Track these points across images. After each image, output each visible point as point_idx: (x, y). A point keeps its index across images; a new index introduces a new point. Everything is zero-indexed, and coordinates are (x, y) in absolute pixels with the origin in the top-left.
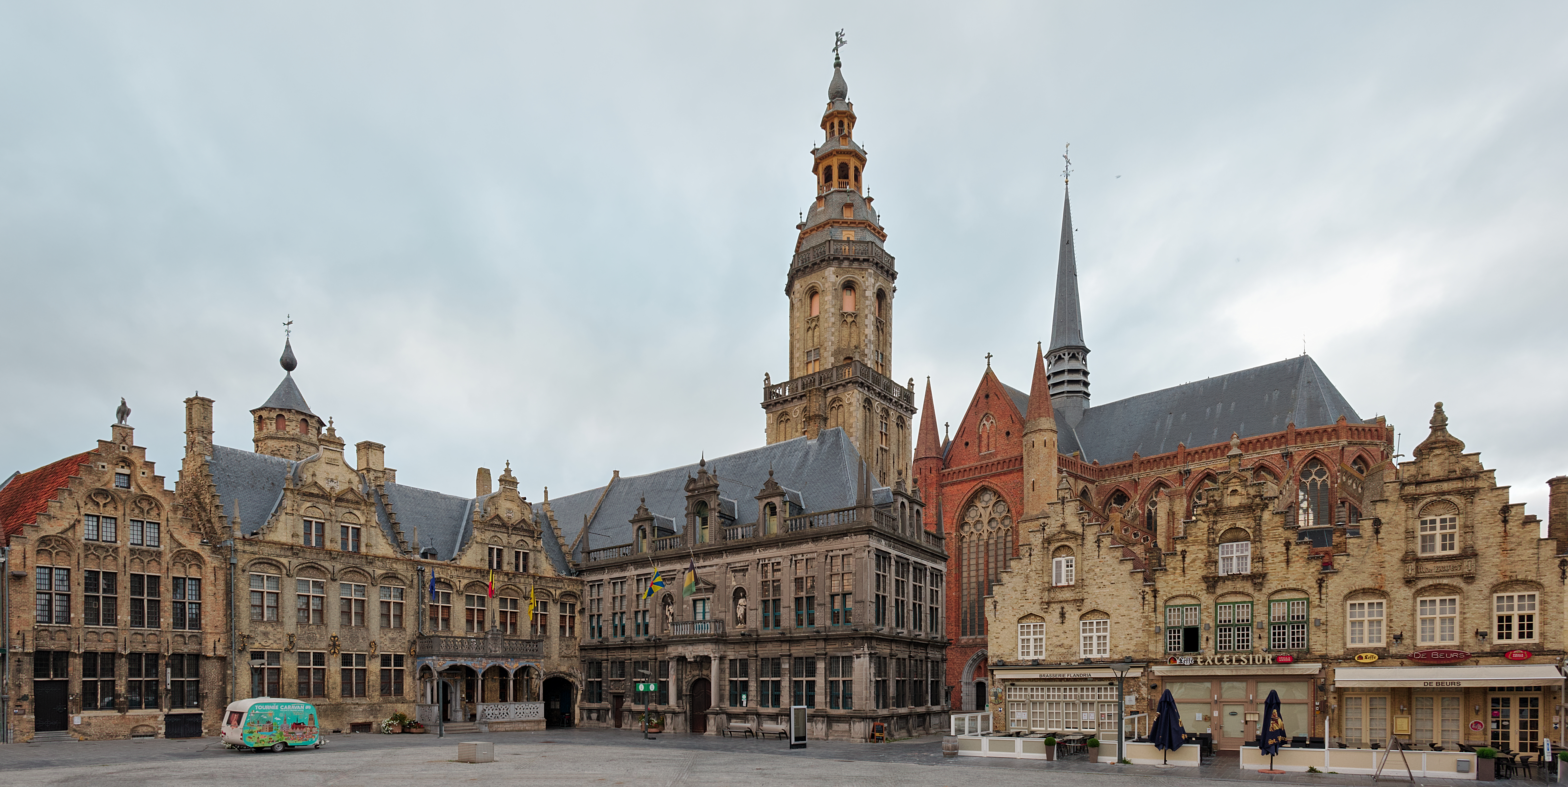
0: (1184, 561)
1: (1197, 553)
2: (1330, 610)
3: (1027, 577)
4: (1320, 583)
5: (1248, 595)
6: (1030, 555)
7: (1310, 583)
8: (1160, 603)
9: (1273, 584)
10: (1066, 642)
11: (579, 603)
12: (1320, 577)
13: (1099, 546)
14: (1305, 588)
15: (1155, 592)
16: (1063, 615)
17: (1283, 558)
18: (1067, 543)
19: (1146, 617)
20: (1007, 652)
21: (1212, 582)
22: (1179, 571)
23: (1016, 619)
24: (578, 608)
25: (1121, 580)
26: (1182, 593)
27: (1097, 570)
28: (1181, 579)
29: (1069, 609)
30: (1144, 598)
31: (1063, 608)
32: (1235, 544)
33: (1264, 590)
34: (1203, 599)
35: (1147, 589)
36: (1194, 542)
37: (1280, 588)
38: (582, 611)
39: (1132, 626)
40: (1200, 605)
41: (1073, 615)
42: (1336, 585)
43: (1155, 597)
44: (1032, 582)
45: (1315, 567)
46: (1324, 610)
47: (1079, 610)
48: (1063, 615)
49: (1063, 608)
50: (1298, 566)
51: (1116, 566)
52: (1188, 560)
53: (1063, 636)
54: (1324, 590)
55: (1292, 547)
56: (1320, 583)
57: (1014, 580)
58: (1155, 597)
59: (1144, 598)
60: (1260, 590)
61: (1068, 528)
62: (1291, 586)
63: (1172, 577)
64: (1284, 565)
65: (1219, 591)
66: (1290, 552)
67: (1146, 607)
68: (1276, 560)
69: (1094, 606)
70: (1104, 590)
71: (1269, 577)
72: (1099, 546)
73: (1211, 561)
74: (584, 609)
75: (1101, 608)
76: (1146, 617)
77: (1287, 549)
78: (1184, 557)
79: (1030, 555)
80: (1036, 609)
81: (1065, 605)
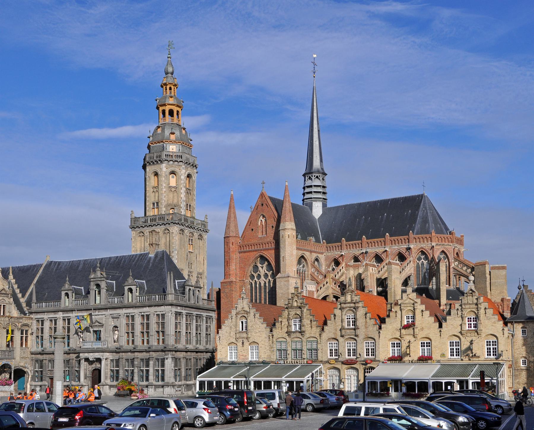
0: (281, 325)
1: (285, 322)
2: (323, 345)
3: (231, 327)
4: (320, 335)
5: (301, 338)
6: (232, 319)
7: (317, 335)
8: (274, 340)
9: (307, 335)
10: (244, 354)
11: (30, 330)
12: (320, 333)
13: (255, 317)
14: (316, 337)
15: (273, 335)
16: (243, 343)
17: (310, 326)
18: (244, 315)
19: (270, 345)
20: (224, 357)
21: (289, 333)
22: (280, 328)
23: (227, 344)
24: (30, 332)
25: (262, 331)
26: (281, 337)
27: (254, 326)
28: (281, 331)
29: (245, 341)
30: (269, 338)
31: (243, 340)
32: (297, 319)
33: (305, 337)
34: (287, 339)
35: (270, 335)
36: (285, 318)
37: (309, 336)
38: (32, 334)
39: (266, 349)
40: (287, 341)
41: (246, 343)
42: (325, 336)
43: (273, 338)
44: (233, 330)
45: (319, 329)
46: (321, 345)
47: (249, 342)
48: (243, 343)
49: (243, 340)
50: (314, 328)
51: (261, 325)
52: (283, 324)
53: (243, 351)
54: (321, 338)
55: (312, 322)
56: (320, 335)
57: (226, 328)
58: (273, 338)
59: (269, 338)
60: (304, 337)
61: (245, 309)
62: (312, 336)
63: (278, 330)
64: (310, 328)
65: (292, 337)
66: (312, 324)
67: (270, 341)
68: (308, 326)
69: (254, 340)
70: (256, 334)
71: (306, 332)
72: (255, 317)
73: (289, 326)
74: (33, 333)
75: (256, 341)
76: (270, 345)
77: (311, 323)
78: (281, 323)
79: (232, 319)
80: (234, 341)
81: (244, 339)
